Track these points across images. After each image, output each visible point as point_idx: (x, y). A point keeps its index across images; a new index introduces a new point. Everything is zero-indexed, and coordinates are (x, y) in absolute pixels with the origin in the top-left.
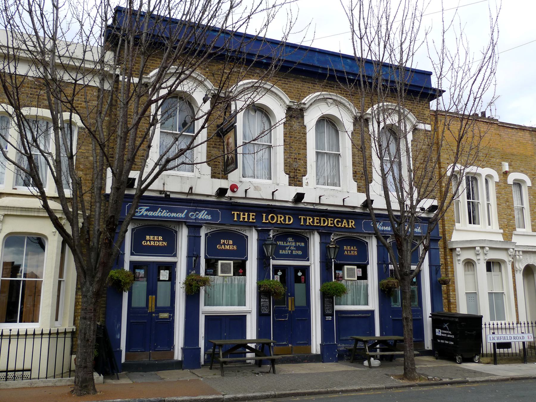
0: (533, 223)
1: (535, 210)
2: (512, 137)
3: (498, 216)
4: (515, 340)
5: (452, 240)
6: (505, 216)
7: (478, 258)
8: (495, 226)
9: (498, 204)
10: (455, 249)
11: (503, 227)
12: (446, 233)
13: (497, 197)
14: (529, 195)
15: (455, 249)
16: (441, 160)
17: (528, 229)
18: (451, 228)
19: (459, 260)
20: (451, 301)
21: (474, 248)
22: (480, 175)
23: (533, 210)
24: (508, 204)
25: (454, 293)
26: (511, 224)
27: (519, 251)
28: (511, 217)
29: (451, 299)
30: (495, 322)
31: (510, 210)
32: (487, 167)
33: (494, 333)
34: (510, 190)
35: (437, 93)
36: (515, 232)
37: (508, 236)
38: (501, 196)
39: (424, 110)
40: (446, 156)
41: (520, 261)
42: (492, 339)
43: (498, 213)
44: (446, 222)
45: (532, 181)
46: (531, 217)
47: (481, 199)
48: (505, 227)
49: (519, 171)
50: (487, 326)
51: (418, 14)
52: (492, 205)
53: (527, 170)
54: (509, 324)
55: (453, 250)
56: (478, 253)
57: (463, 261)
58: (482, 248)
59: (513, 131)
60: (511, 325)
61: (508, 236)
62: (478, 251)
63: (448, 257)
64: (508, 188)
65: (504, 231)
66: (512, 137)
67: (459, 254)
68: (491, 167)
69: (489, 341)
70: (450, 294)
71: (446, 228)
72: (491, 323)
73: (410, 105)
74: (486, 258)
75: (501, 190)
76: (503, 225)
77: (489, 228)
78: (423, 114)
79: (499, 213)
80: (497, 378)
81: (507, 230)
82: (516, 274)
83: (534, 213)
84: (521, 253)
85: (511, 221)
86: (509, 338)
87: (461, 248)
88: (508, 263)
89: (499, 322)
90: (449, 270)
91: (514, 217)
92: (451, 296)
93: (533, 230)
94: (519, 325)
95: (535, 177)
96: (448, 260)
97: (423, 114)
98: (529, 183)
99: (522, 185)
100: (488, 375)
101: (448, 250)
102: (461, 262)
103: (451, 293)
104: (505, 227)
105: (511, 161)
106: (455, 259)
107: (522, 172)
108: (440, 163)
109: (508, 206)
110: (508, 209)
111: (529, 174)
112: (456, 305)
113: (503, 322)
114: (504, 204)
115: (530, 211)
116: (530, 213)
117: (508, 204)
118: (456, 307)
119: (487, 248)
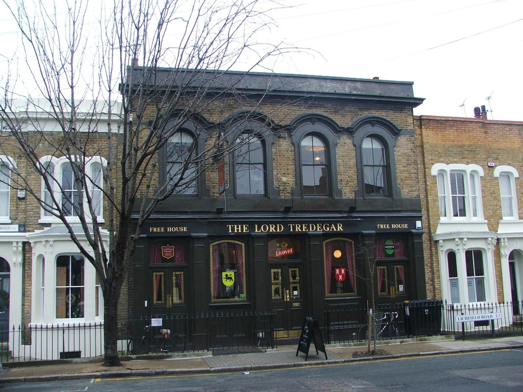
0: (520, 211)
1: (522, 199)
2: (499, 133)
3: (483, 208)
4: (466, 320)
5: (437, 233)
6: (490, 207)
7: (458, 248)
8: (480, 218)
9: (483, 197)
10: (439, 241)
11: (488, 217)
12: (431, 227)
13: (482, 191)
14: (516, 186)
15: (439, 241)
16: (426, 161)
17: (515, 218)
18: (436, 222)
19: (442, 251)
20: (436, 287)
21: (454, 239)
22: (464, 171)
23: (520, 200)
24: (494, 195)
25: (439, 280)
26: (497, 214)
27: (504, 239)
28: (498, 207)
29: (436, 285)
30: (475, 304)
31: (497, 201)
32: (472, 163)
33: (462, 314)
34: (497, 183)
35: (419, 101)
36: (501, 221)
37: (493, 227)
38: (486, 189)
39: (407, 117)
40: (430, 157)
41: (505, 247)
42: (460, 319)
43: (483, 205)
44: (430, 217)
45: (519, 173)
46: (518, 206)
47: (468, 194)
48: (491, 217)
49: (506, 163)
50: (467, 307)
51: (299, 50)
52: (478, 199)
53: (514, 162)
54: (488, 304)
55: (437, 242)
56: (457, 244)
57: (446, 251)
58: (461, 239)
59: (500, 127)
60: (490, 306)
61: (493, 227)
62: (457, 242)
63: (433, 248)
64: (494, 180)
65: (489, 221)
66: (499, 133)
67: (441, 245)
68: (476, 163)
69: (457, 321)
70: (435, 281)
71: (431, 222)
72: (471, 304)
73: (392, 114)
74: (465, 248)
75: (486, 183)
76: (488, 215)
77: (475, 219)
78: (405, 121)
79: (485, 205)
80: (451, 351)
81: (492, 219)
82: (501, 259)
83: (521, 202)
84: (506, 240)
85: (498, 211)
86: (477, 317)
87: (444, 240)
88: (487, 251)
89: (479, 303)
90: (434, 260)
91: (501, 207)
92: (436, 283)
93: (520, 218)
94: (502, 305)
95: (522, 168)
96: (433, 251)
97: (405, 121)
98: (516, 174)
99: (510, 176)
100: (451, 349)
101: (432, 242)
102: (444, 252)
103: (436, 280)
104: (491, 217)
105: (498, 155)
106: (440, 249)
107: (509, 164)
108: (424, 164)
109: (495, 197)
110: (494, 200)
111: (516, 166)
112: (440, 290)
113: (482, 303)
114: (490, 197)
115: (518, 200)
116: (518, 202)
117: (494, 195)
118: (440, 292)
119: (465, 239)
